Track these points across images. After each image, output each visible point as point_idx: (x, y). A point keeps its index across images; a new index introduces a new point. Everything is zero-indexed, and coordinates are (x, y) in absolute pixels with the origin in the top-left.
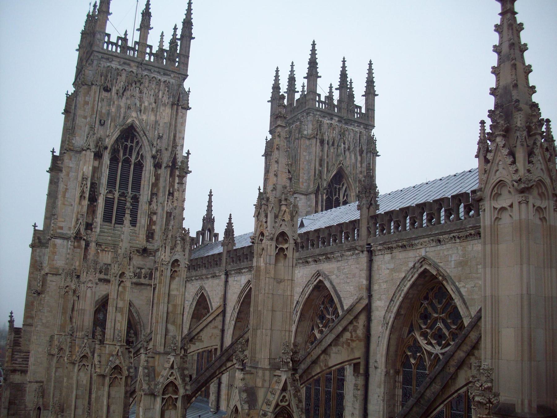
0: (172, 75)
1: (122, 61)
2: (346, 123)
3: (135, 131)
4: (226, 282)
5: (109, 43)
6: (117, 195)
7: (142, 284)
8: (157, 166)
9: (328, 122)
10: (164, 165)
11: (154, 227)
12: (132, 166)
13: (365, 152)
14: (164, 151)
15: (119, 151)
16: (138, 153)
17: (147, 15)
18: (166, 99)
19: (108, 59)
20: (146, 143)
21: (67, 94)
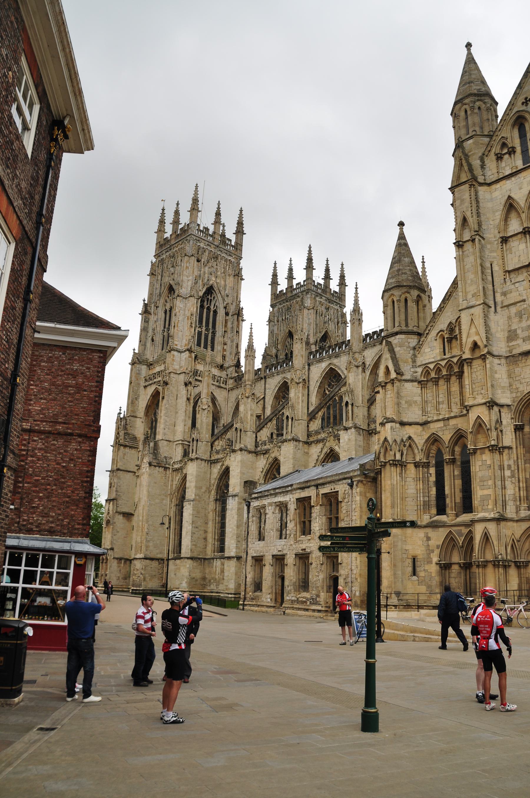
0: (234, 257)
1: (207, 243)
2: (329, 302)
3: (213, 290)
4: (309, 369)
5: (199, 230)
6: (204, 328)
7: (222, 387)
8: (227, 314)
9: (319, 300)
10: (230, 314)
11: (225, 353)
12: (212, 313)
13: (340, 322)
14: (230, 304)
15: (204, 301)
16: (215, 305)
17: (218, 214)
18: (230, 272)
19: (199, 241)
20: (220, 298)
21: (152, 262)
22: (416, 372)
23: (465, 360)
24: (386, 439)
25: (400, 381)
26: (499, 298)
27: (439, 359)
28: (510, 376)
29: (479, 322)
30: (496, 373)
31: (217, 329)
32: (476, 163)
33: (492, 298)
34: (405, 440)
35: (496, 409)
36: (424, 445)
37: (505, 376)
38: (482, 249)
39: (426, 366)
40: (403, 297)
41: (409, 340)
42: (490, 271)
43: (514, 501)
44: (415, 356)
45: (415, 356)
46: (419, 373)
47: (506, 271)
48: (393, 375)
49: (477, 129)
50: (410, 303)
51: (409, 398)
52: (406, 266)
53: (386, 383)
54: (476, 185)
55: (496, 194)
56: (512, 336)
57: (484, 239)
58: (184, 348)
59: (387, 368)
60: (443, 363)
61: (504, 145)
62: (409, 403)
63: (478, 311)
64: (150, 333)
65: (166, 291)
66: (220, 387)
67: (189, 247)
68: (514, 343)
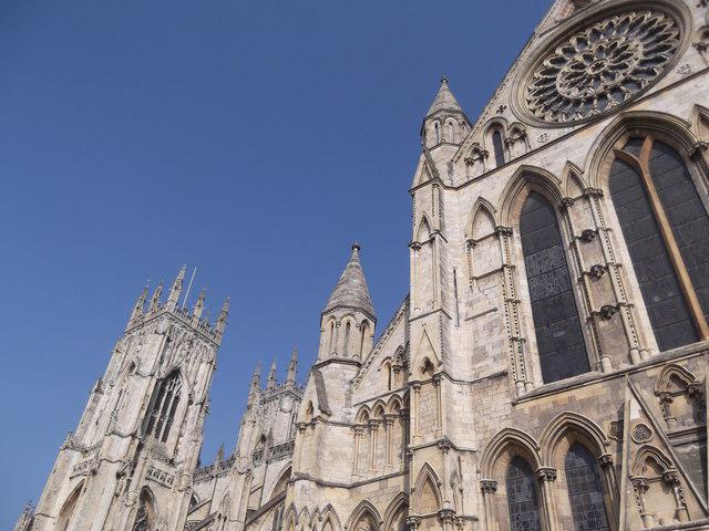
8: (190, 402)
12: (173, 399)
23: (413, 383)
24: (292, 504)
25: (325, 422)
26: (463, 309)
27: (381, 394)
28: (475, 410)
29: (434, 334)
34: (321, 509)
36: (348, 521)
37: (468, 409)
38: (443, 250)
39: (363, 404)
40: (345, 319)
41: (345, 371)
42: (452, 278)
45: (351, 392)
46: (354, 416)
47: (473, 278)
48: (317, 413)
50: (353, 327)
51: (337, 449)
53: (306, 425)
55: (465, 197)
56: (479, 355)
58: (128, 432)
59: (311, 404)
60: (386, 399)
62: (335, 456)
63: (433, 320)
64: (97, 414)
65: (126, 370)
66: (162, 485)
67: (164, 325)
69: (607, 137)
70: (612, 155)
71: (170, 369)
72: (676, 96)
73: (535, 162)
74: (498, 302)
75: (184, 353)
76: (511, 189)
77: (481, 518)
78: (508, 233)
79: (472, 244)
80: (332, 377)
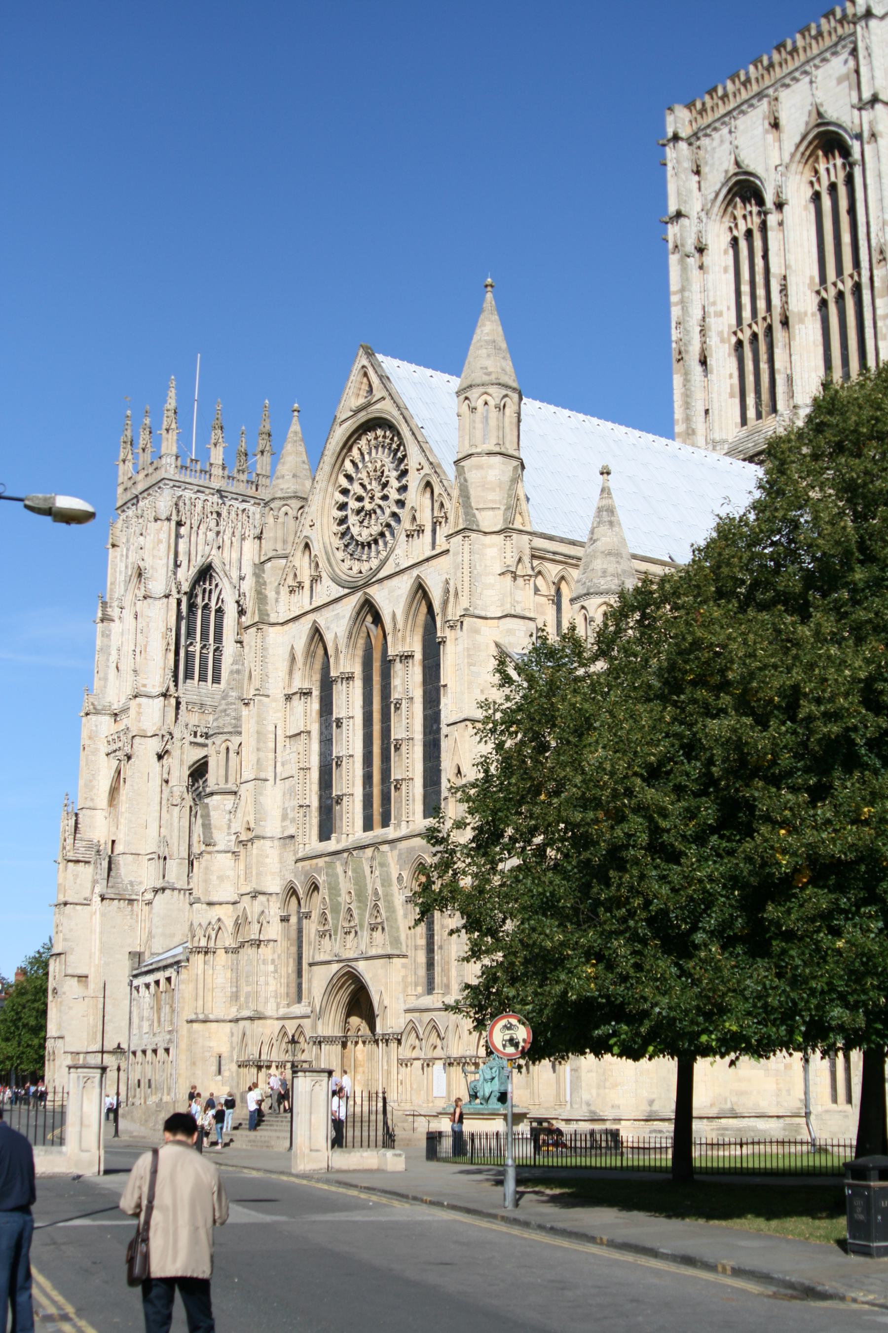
0: (252, 501)
1: (196, 488)
6: (198, 646)
22: (230, 841)
25: (209, 853)
30: (267, 857)
31: (224, 643)
32: (271, 594)
33: (271, 769)
34: (213, 922)
35: (261, 898)
37: (276, 860)
40: (224, 746)
43: (276, 997)
44: (230, 820)
49: (279, 546)
50: (232, 755)
52: (232, 704)
54: (265, 627)
56: (284, 817)
57: (268, 696)
61: (295, 575)
62: (221, 878)
68: (285, 824)
69: (358, 614)
70: (364, 629)
71: (193, 571)
72: (390, 592)
73: (322, 619)
74: (294, 771)
75: (211, 535)
76: (310, 644)
77: (279, 940)
78: (307, 694)
79: (288, 698)
80: (216, 808)
